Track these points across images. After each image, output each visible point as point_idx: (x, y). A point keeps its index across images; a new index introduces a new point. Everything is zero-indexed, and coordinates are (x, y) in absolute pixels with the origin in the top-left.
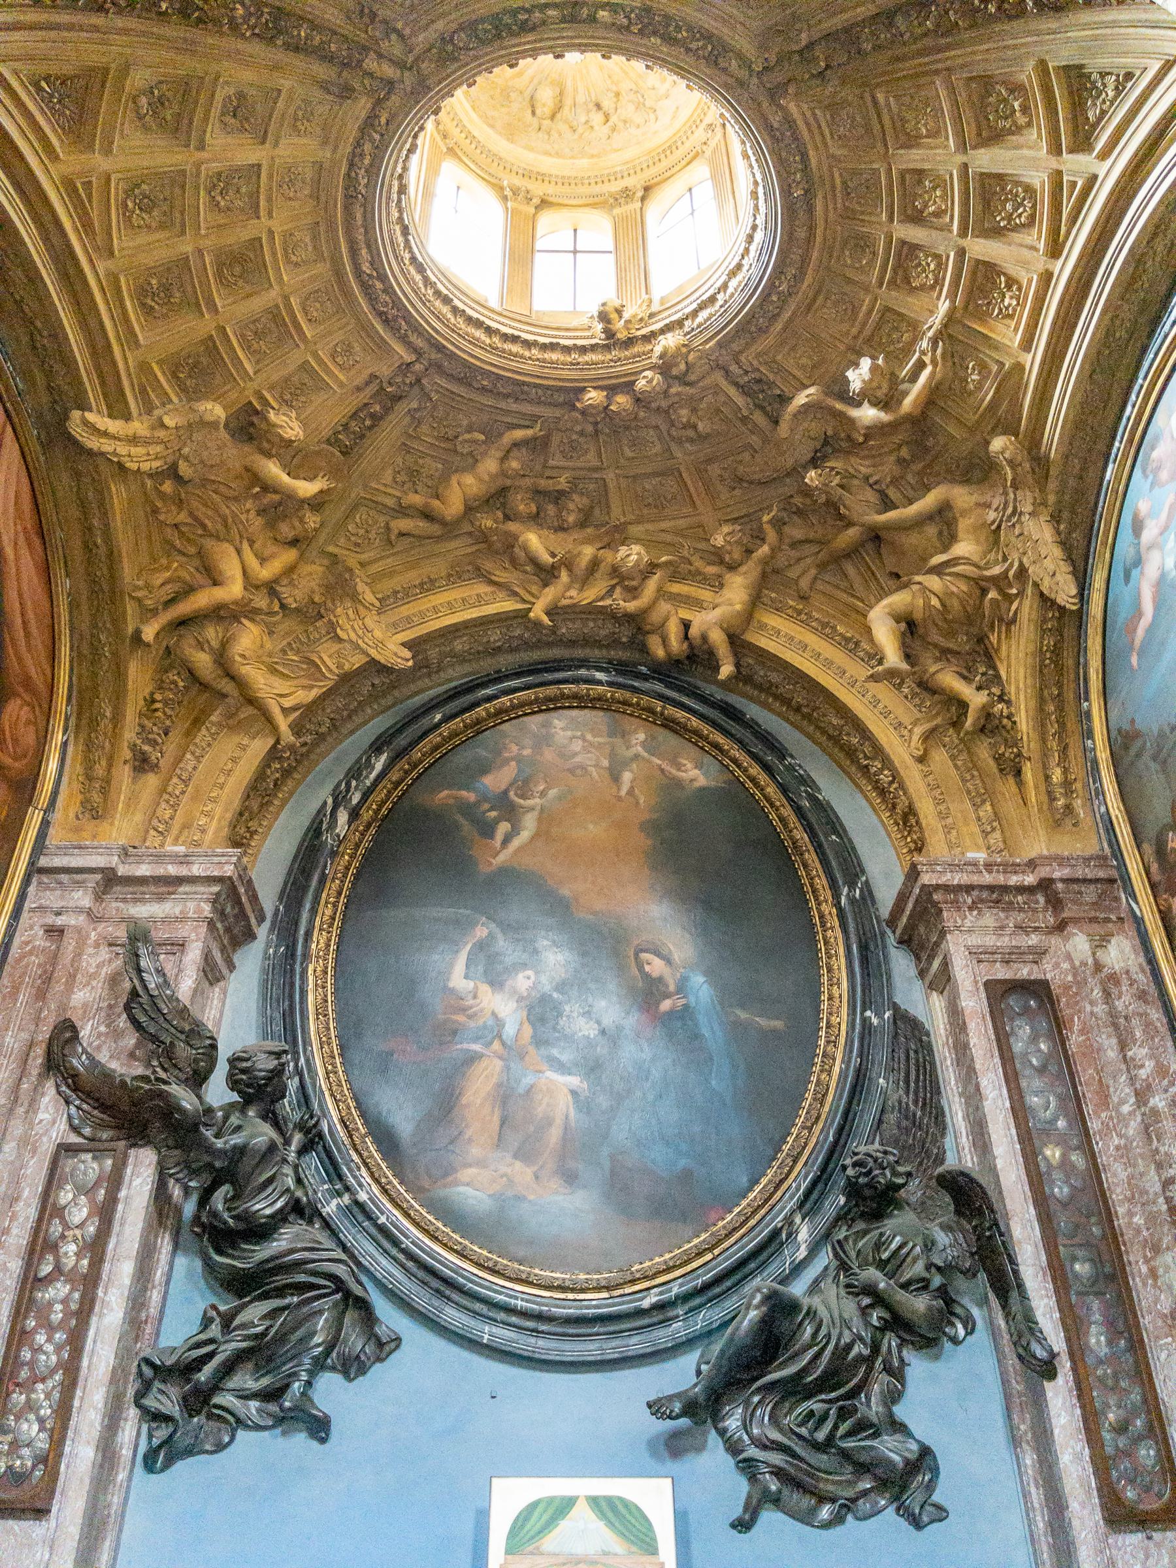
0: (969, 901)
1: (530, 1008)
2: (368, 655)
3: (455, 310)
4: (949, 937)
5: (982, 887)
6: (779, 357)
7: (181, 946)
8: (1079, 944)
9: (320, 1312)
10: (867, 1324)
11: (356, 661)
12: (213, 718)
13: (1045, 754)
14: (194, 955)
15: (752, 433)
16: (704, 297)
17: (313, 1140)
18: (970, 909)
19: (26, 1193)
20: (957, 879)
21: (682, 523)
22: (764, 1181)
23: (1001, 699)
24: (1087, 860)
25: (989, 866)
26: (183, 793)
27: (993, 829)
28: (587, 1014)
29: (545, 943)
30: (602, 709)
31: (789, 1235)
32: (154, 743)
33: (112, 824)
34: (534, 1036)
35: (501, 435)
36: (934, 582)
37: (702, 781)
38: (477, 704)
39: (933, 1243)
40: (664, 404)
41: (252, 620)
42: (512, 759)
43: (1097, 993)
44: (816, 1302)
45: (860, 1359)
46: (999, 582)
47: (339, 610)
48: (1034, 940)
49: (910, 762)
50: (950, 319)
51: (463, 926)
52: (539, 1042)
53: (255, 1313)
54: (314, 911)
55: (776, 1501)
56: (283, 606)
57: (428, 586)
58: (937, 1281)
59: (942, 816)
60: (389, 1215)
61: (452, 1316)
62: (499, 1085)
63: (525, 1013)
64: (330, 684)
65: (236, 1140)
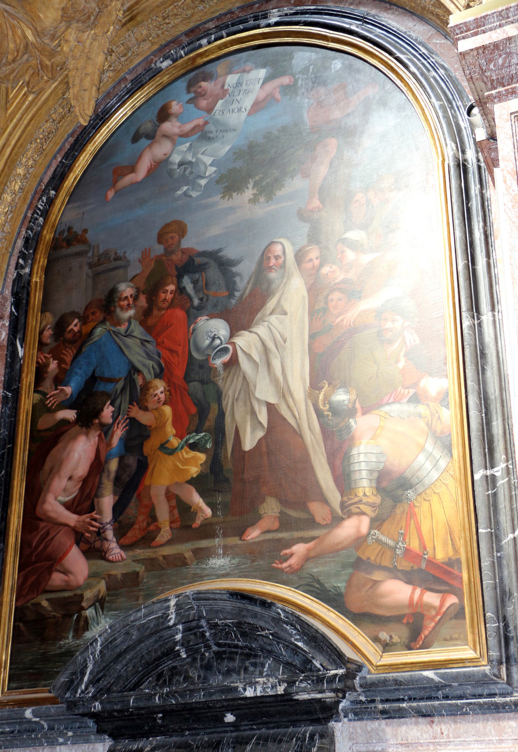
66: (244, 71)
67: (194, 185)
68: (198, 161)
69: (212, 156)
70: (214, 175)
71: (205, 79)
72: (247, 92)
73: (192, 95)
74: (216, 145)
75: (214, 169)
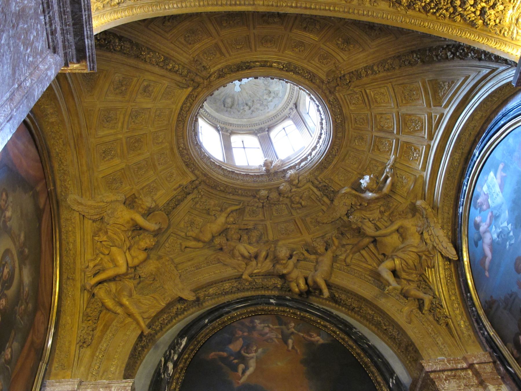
6: (332, 178)
15: (323, 205)
16: (303, 158)
21: (297, 240)
35: (226, 209)
37: (321, 341)
38: (222, 315)
40: (290, 195)
42: (240, 337)
50: (395, 160)
66: (486, 181)
67: (510, 238)
68: (502, 228)
69: (505, 221)
70: (512, 227)
71: (477, 199)
72: (494, 186)
73: (479, 209)
74: (502, 216)
75: (510, 225)
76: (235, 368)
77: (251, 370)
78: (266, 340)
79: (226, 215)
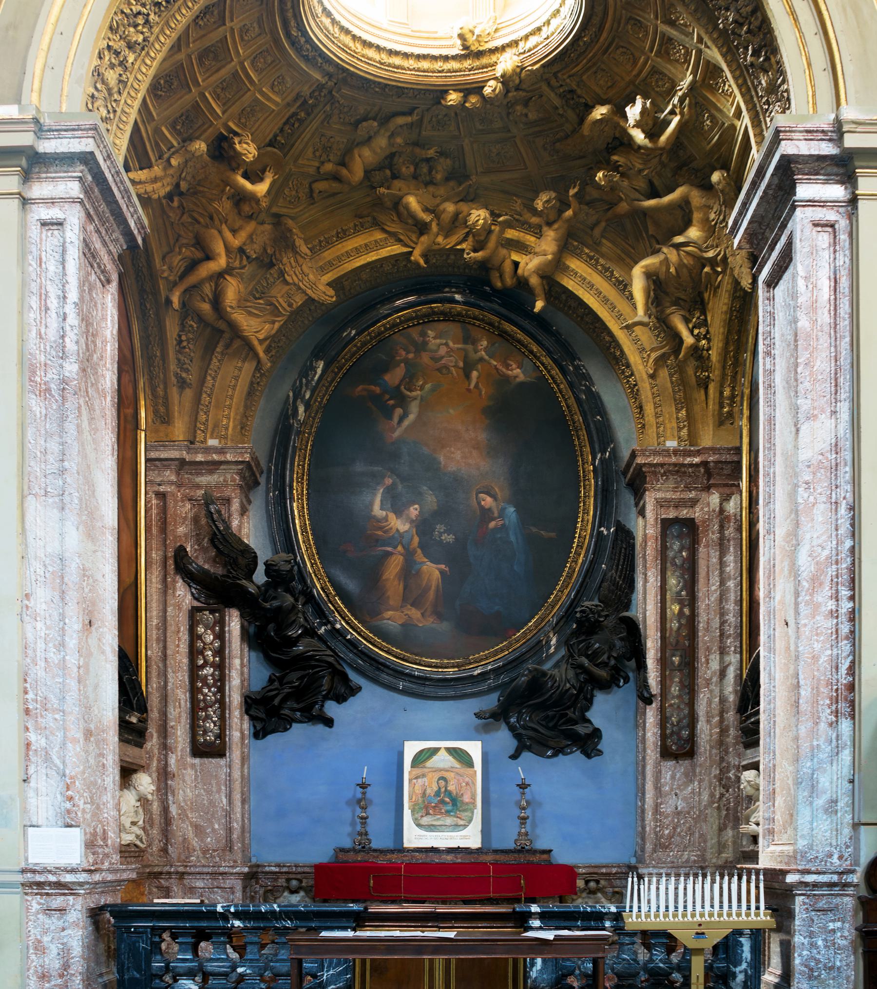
0: (662, 471)
1: (417, 527)
2: (307, 295)
3: (354, 37)
4: (647, 493)
5: (669, 464)
7: (228, 501)
8: (715, 499)
9: (324, 677)
10: (578, 680)
11: (299, 300)
12: (218, 350)
13: (723, 376)
14: (236, 505)
17: (310, 598)
18: (662, 476)
19: (182, 629)
20: (656, 460)
22: (537, 617)
23: (705, 337)
24: (729, 449)
25: (676, 452)
26: (210, 403)
27: (684, 426)
28: (447, 531)
29: (425, 488)
30: (459, 321)
31: (547, 642)
32: (187, 371)
33: (174, 427)
34: (419, 543)
36: (672, 255)
39: (614, 646)
41: (231, 275)
43: (716, 527)
44: (555, 672)
45: (573, 695)
46: (712, 262)
47: (285, 260)
48: (692, 495)
49: (645, 376)
51: (377, 478)
52: (421, 546)
53: (294, 677)
54: (292, 471)
55: (529, 749)
56: (248, 257)
57: (342, 235)
58: (613, 662)
59: (657, 415)
60: (352, 635)
61: (385, 677)
62: (402, 569)
63: (414, 530)
64: (285, 318)
65: (276, 603)
76: (388, 413)
77: (412, 417)
78: (439, 370)
79: (388, 134)
